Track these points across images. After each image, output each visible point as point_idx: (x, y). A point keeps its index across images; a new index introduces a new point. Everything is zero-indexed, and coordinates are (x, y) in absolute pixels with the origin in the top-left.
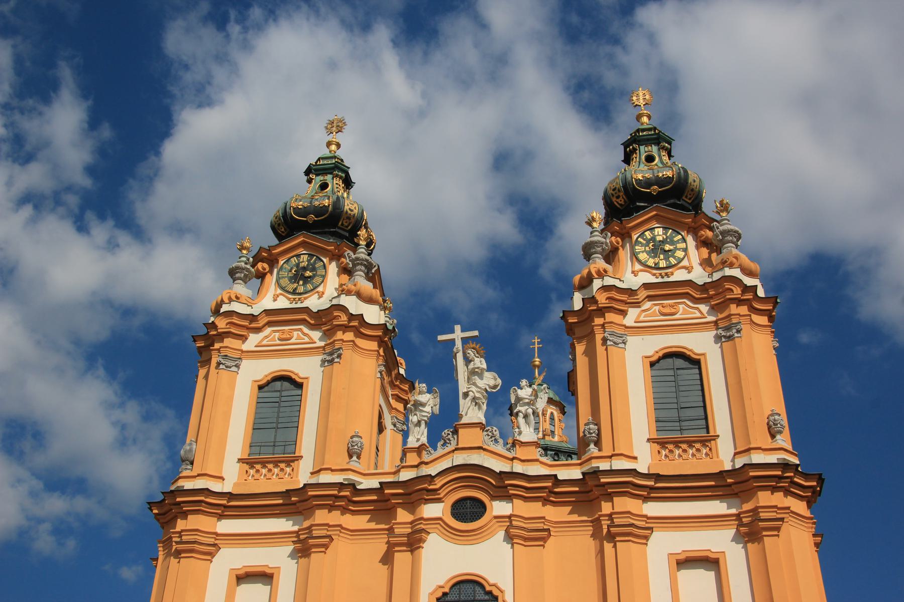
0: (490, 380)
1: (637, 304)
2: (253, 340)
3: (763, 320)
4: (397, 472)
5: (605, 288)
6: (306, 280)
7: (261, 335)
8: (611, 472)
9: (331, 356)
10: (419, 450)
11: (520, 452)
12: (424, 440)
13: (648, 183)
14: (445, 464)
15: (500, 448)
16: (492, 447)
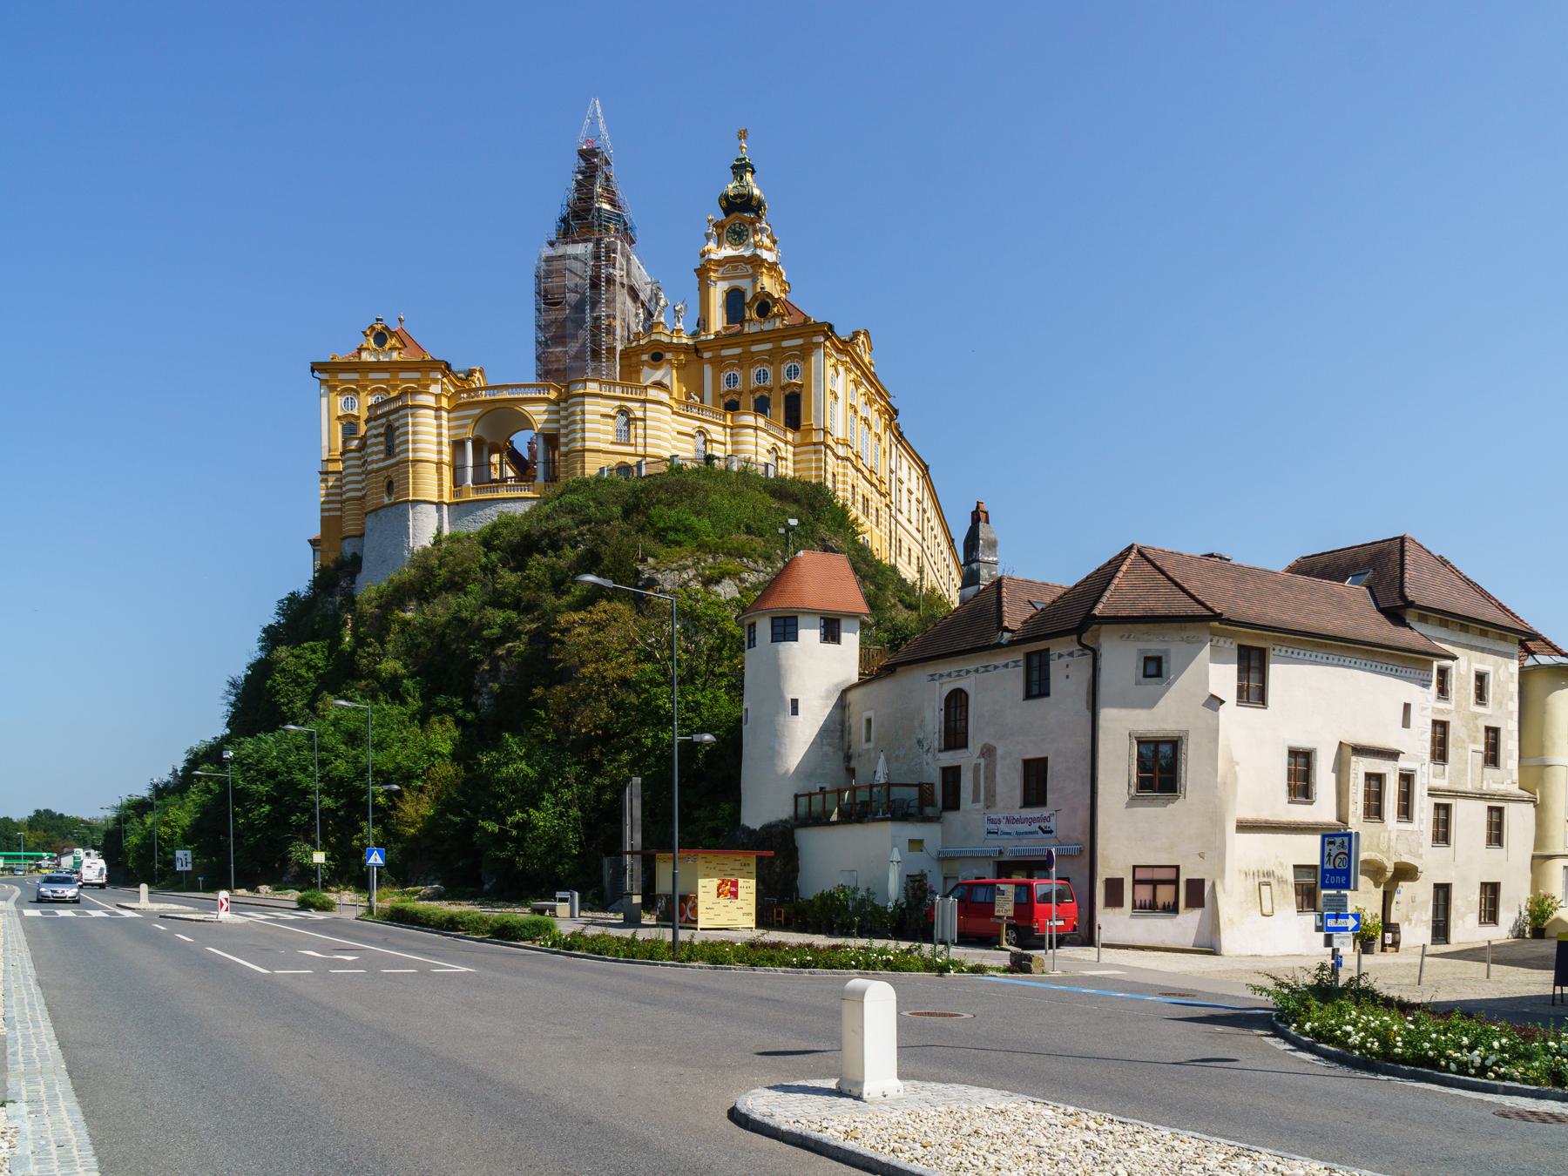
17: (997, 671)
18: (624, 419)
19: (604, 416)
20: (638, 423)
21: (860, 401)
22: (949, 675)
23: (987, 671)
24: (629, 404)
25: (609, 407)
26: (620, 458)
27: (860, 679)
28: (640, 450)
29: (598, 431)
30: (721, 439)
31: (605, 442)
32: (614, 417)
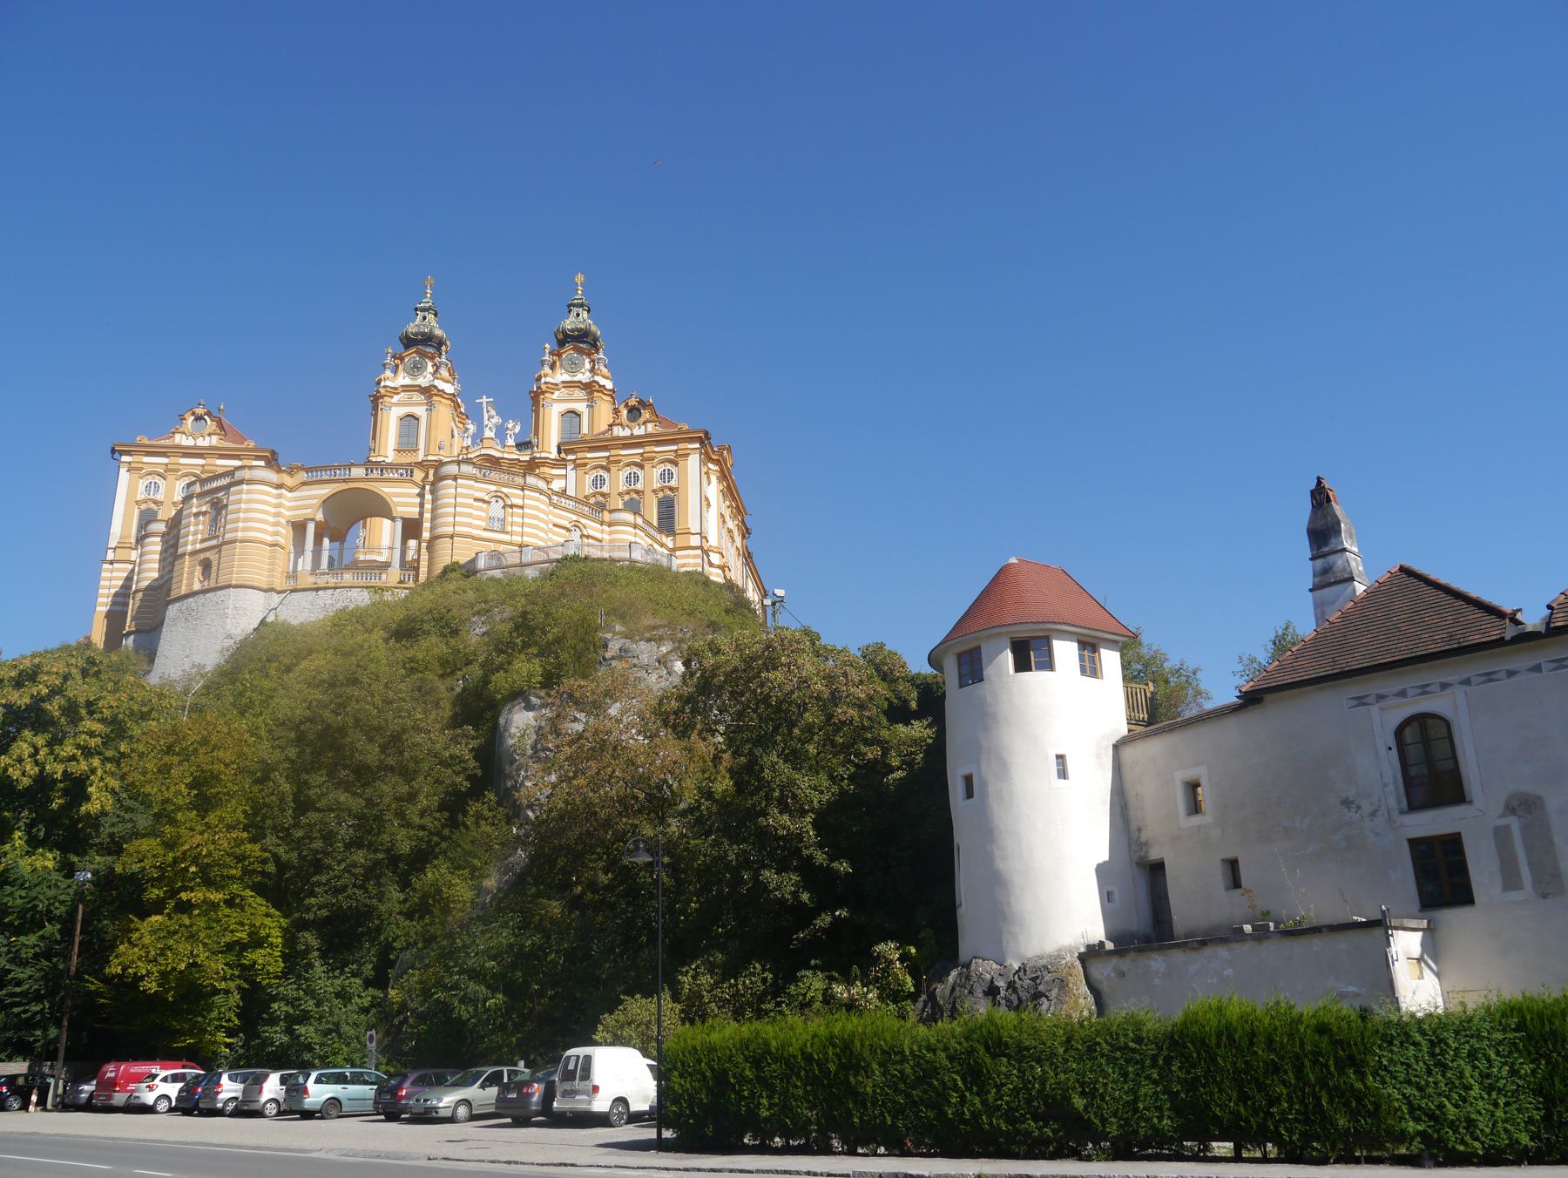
0: (497, 420)
1: (558, 390)
2: (396, 399)
3: (609, 398)
4: (458, 456)
5: (546, 383)
6: (418, 368)
7: (399, 396)
8: (540, 458)
9: (430, 407)
10: (467, 448)
11: (507, 449)
12: (470, 443)
13: (572, 330)
14: (478, 453)
15: (499, 448)
16: (496, 447)
17: (1515, 679)
18: (501, 503)
19: (476, 500)
20: (515, 510)
21: (727, 513)
22: (1403, 694)
23: (1491, 680)
24: (505, 490)
25: (483, 490)
26: (493, 546)
27: (1129, 731)
28: (517, 539)
29: (470, 515)
30: (599, 536)
31: (477, 527)
32: (489, 503)
